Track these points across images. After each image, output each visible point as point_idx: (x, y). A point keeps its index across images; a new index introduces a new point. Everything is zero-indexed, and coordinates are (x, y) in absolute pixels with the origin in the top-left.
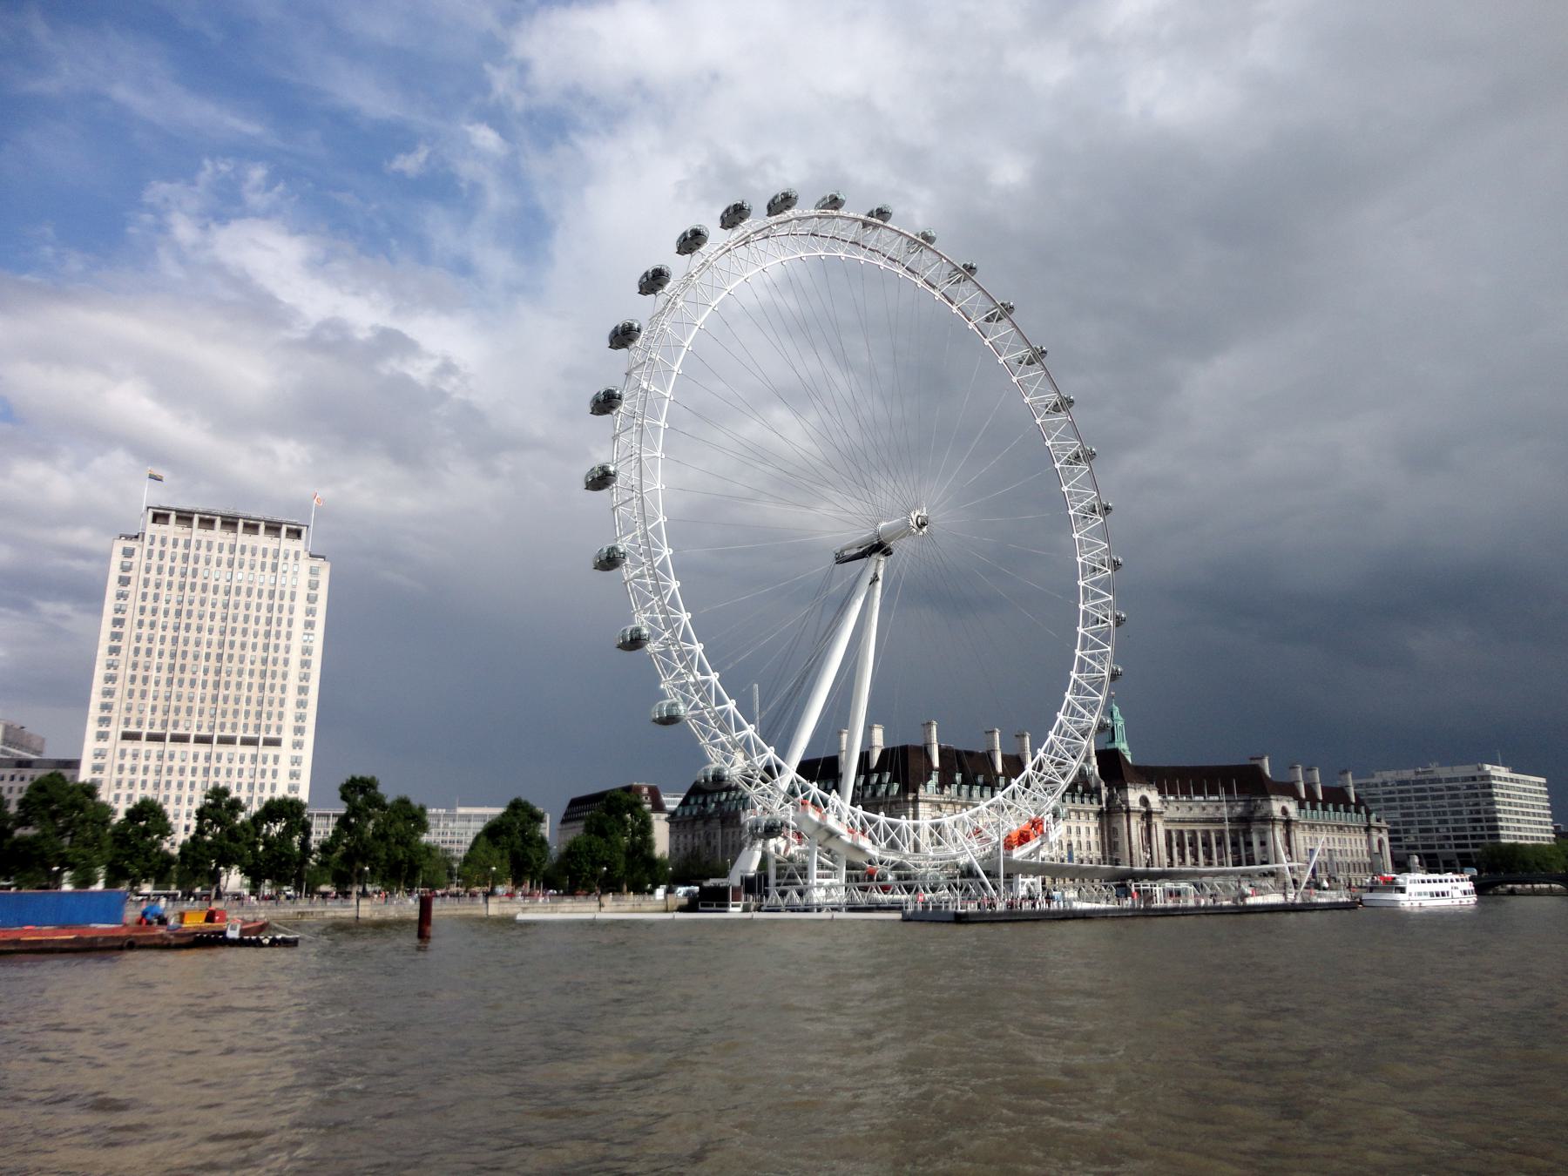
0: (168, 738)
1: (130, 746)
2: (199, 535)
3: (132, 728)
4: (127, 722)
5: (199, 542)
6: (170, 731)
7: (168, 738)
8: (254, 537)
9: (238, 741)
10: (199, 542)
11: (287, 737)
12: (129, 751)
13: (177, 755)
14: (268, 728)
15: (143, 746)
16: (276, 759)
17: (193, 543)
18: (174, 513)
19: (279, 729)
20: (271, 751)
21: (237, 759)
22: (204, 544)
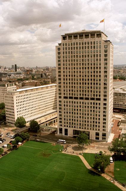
0: (73, 98)
1: (66, 100)
2: (74, 41)
3: (66, 96)
4: (64, 94)
5: (74, 43)
6: (74, 96)
7: (73, 98)
8: (88, 39)
9: (90, 99)
10: (74, 43)
11: (102, 98)
12: (66, 102)
13: (76, 102)
14: (97, 95)
15: (69, 100)
16: (99, 104)
17: (73, 44)
18: (67, 36)
19: (100, 95)
20: (98, 102)
21: (90, 104)
22: (76, 44)
